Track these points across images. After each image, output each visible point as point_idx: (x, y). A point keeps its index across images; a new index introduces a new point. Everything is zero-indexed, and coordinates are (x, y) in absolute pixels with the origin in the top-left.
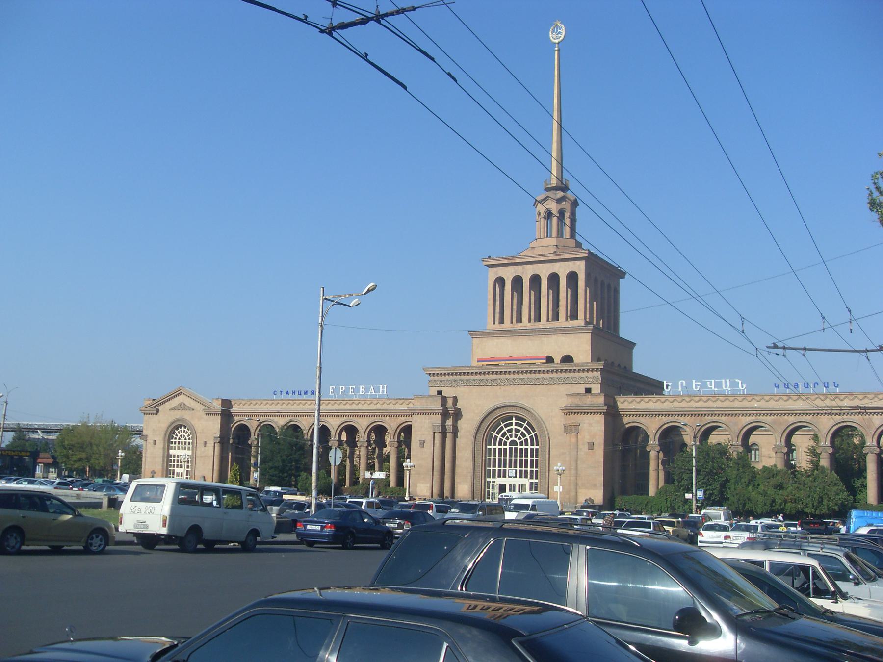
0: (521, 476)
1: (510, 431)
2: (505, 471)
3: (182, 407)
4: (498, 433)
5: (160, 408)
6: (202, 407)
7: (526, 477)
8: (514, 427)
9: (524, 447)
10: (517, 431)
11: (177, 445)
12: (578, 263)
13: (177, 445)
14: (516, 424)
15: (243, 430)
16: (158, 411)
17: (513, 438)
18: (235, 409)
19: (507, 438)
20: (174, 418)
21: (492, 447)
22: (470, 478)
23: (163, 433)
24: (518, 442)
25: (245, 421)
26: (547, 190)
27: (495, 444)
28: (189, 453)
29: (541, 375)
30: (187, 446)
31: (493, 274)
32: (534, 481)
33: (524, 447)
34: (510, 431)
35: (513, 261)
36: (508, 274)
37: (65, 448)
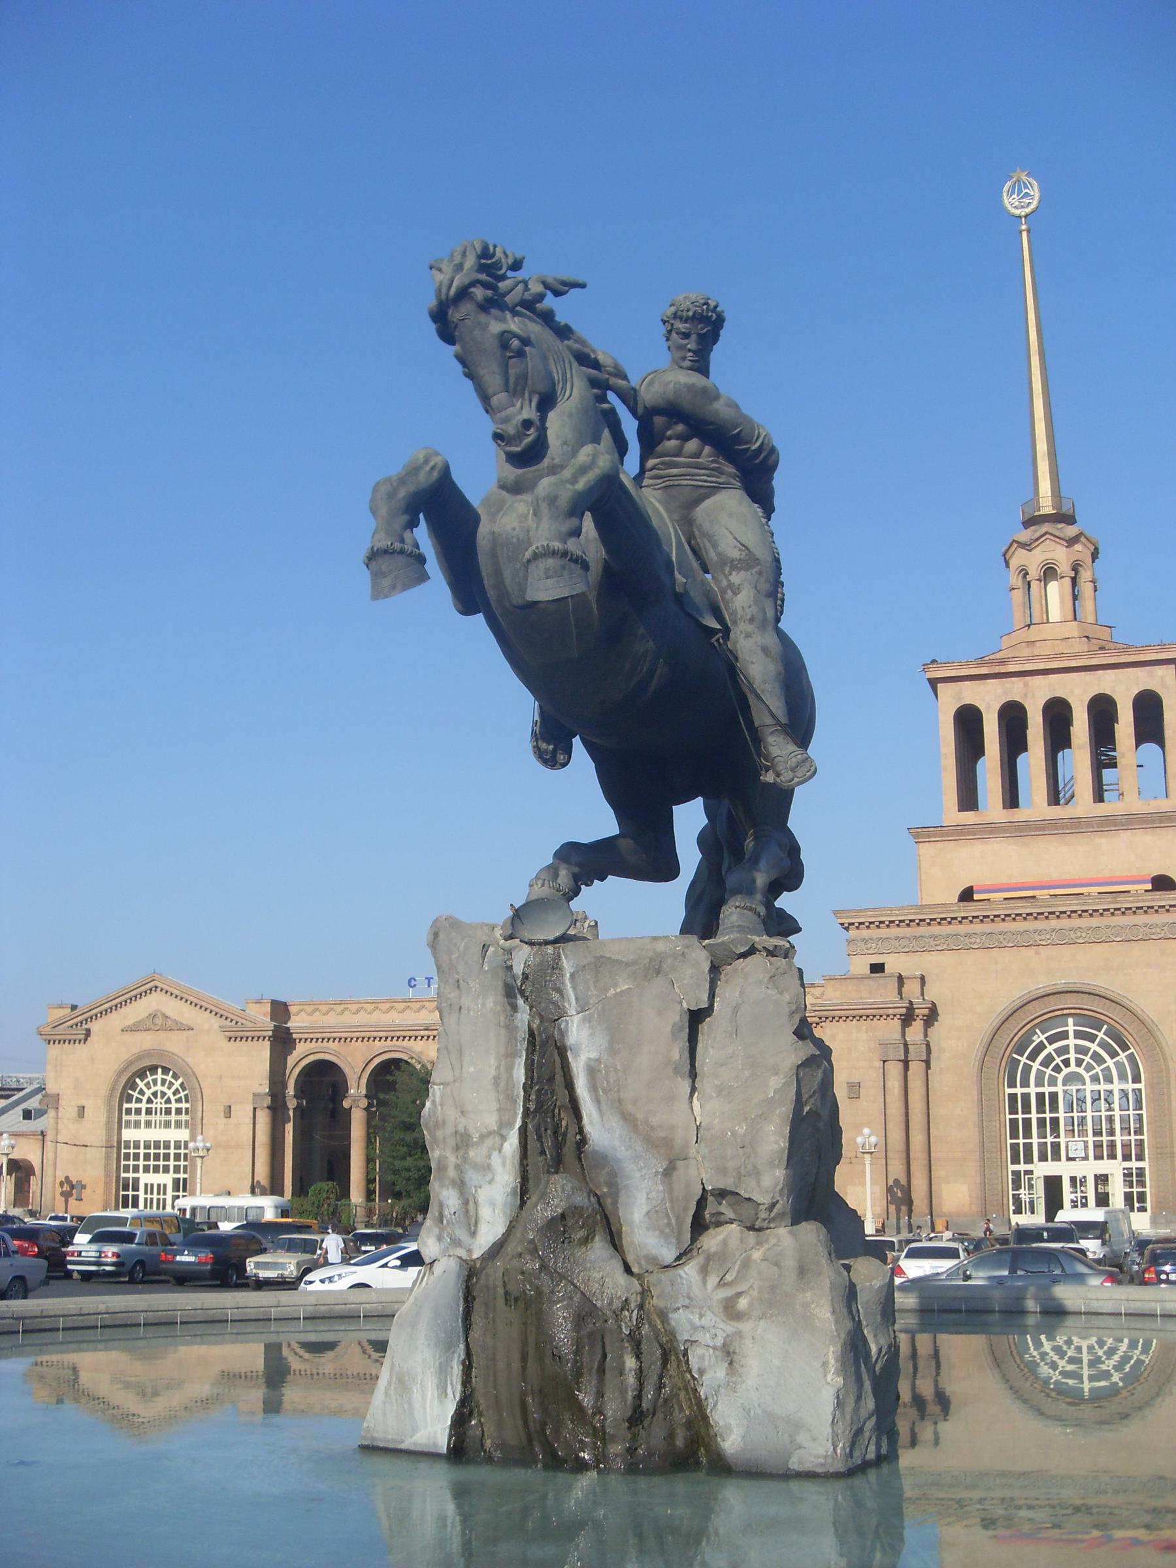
0: (1099, 1157)
1: (1064, 1050)
2: (1056, 1147)
3: (157, 1023)
4: (1033, 1057)
5: (95, 1026)
6: (216, 1022)
7: (1113, 1156)
8: (1072, 1042)
9: (1103, 1087)
10: (1080, 1050)
11: (143, 1117)
12: (1159, 671)
13: (143, 1117)
14: (1078, 1035)
15: (323, 1079)
16: (88, 1033)
17: (1073, 1068)
18: (296, 1023)
19: (1057, 1069)
20: (136, 1050)
21: (1019, 1090)
22: (972, 1167)
23: (104, 1091)
24: (1087, 1076)
25: (331, 1052)
26: (1029, 522)
27: (1026, 1084)
28: (183, 1135)
29: (1140, 919)
30: (173, 1117)
31: (951, 699)
32: (1134, 1164)
33: (1103, 1087)
34: (1064, 1050)
35: (1003, 669)
36: (989, 699)
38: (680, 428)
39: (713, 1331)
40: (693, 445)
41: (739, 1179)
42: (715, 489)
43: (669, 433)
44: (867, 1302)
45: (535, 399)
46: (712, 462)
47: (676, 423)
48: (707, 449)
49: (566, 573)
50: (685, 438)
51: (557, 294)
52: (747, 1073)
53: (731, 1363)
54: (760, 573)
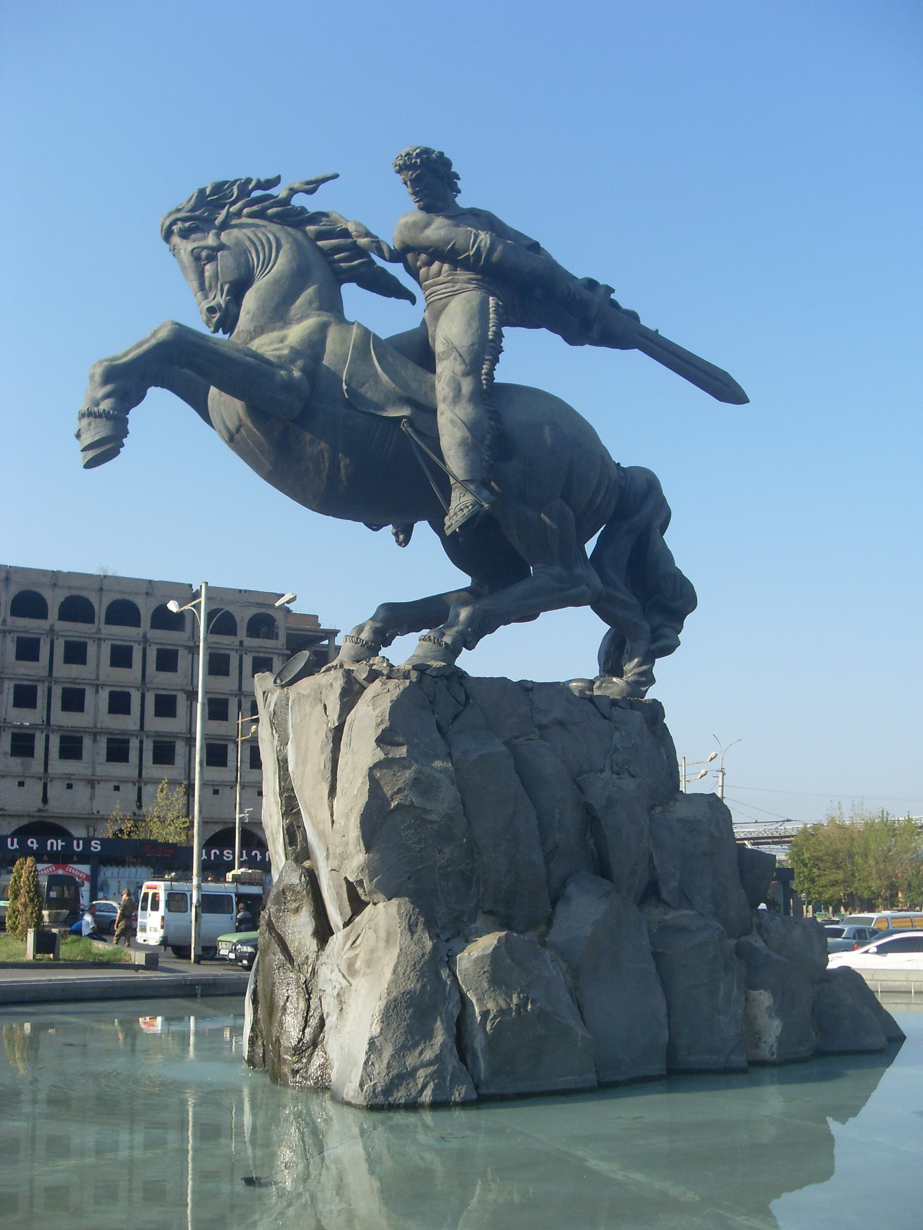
37: (805, 865)
38: (423, 257)
39: (334, 984)
40: (436, 265)
41: (342, 863)
42: (454, 294)
43: (419, 263)
44: (466, 969)
45: (226, 288)
46: (448, 276)
47: (419, 255)
48: (446, 267)
49: (92, 427)
50: (429, 264)
51: (310, 192)
52: (352, 776)
53: (341, 1010)
54: (455, 359)
